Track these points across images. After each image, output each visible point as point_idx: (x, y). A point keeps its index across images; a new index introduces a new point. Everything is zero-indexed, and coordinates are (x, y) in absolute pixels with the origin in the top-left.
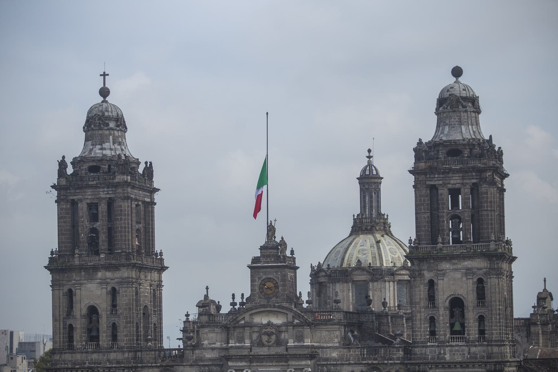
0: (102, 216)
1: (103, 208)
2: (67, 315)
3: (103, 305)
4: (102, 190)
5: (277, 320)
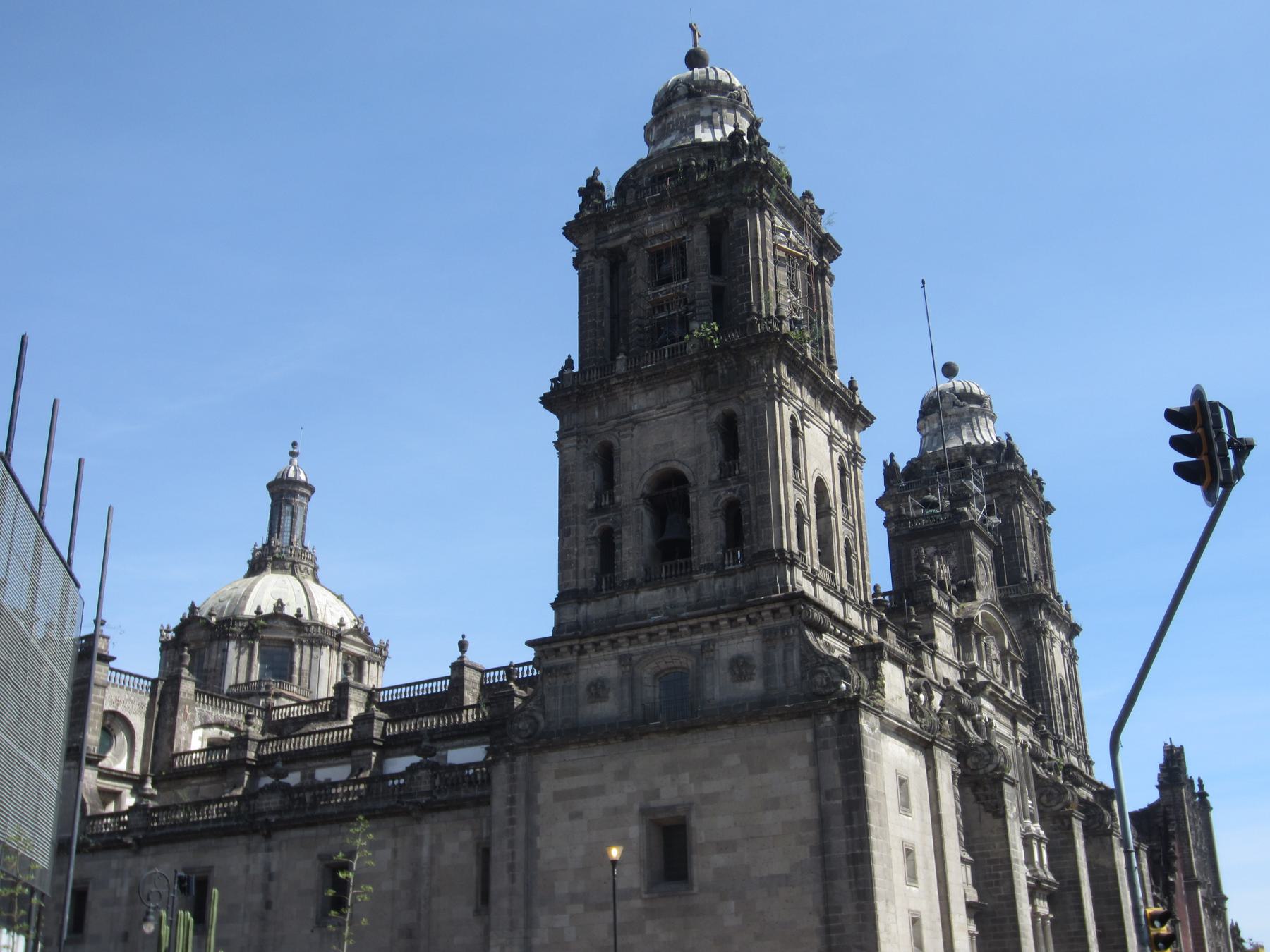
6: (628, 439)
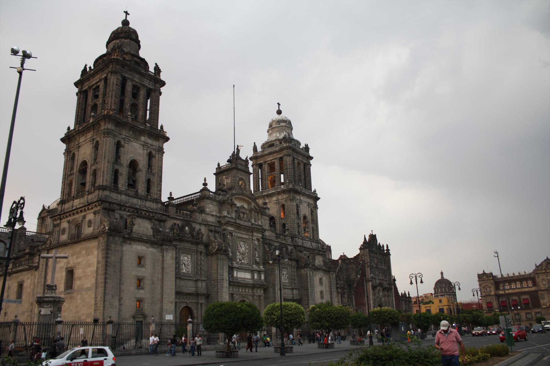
1: (142, 93)
2: (115, 161)
3: (142, 163)
4: (146, 80)
5: (246, 206)
6: (77, 152)
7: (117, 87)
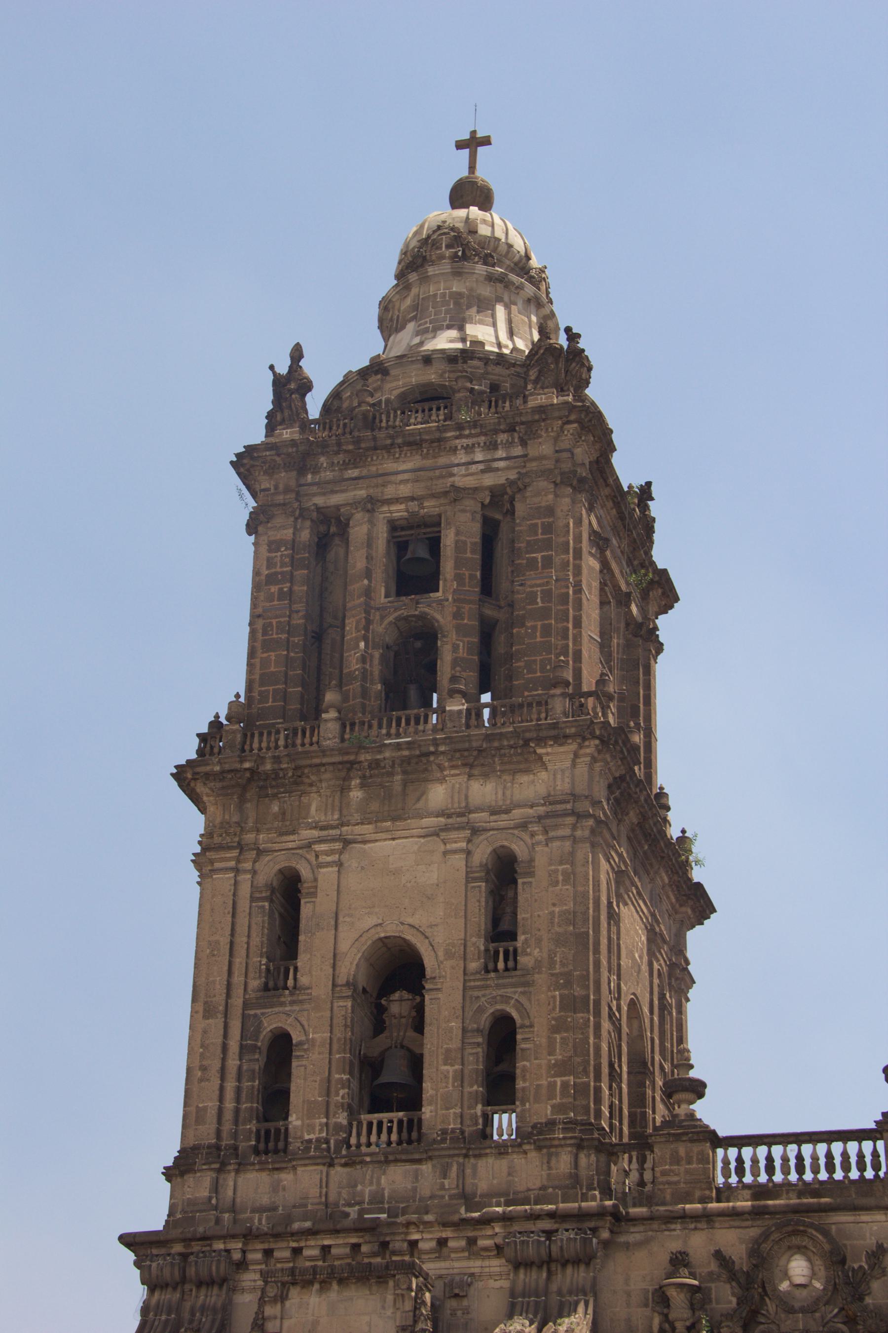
0: (458, 563)
2: (266, 988)
4: (462, 457)
7: (274, 589)
